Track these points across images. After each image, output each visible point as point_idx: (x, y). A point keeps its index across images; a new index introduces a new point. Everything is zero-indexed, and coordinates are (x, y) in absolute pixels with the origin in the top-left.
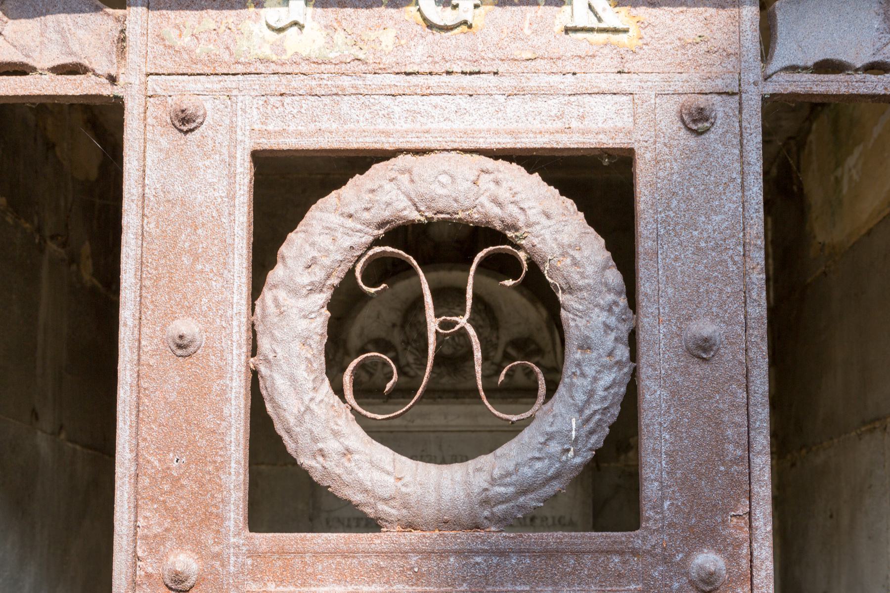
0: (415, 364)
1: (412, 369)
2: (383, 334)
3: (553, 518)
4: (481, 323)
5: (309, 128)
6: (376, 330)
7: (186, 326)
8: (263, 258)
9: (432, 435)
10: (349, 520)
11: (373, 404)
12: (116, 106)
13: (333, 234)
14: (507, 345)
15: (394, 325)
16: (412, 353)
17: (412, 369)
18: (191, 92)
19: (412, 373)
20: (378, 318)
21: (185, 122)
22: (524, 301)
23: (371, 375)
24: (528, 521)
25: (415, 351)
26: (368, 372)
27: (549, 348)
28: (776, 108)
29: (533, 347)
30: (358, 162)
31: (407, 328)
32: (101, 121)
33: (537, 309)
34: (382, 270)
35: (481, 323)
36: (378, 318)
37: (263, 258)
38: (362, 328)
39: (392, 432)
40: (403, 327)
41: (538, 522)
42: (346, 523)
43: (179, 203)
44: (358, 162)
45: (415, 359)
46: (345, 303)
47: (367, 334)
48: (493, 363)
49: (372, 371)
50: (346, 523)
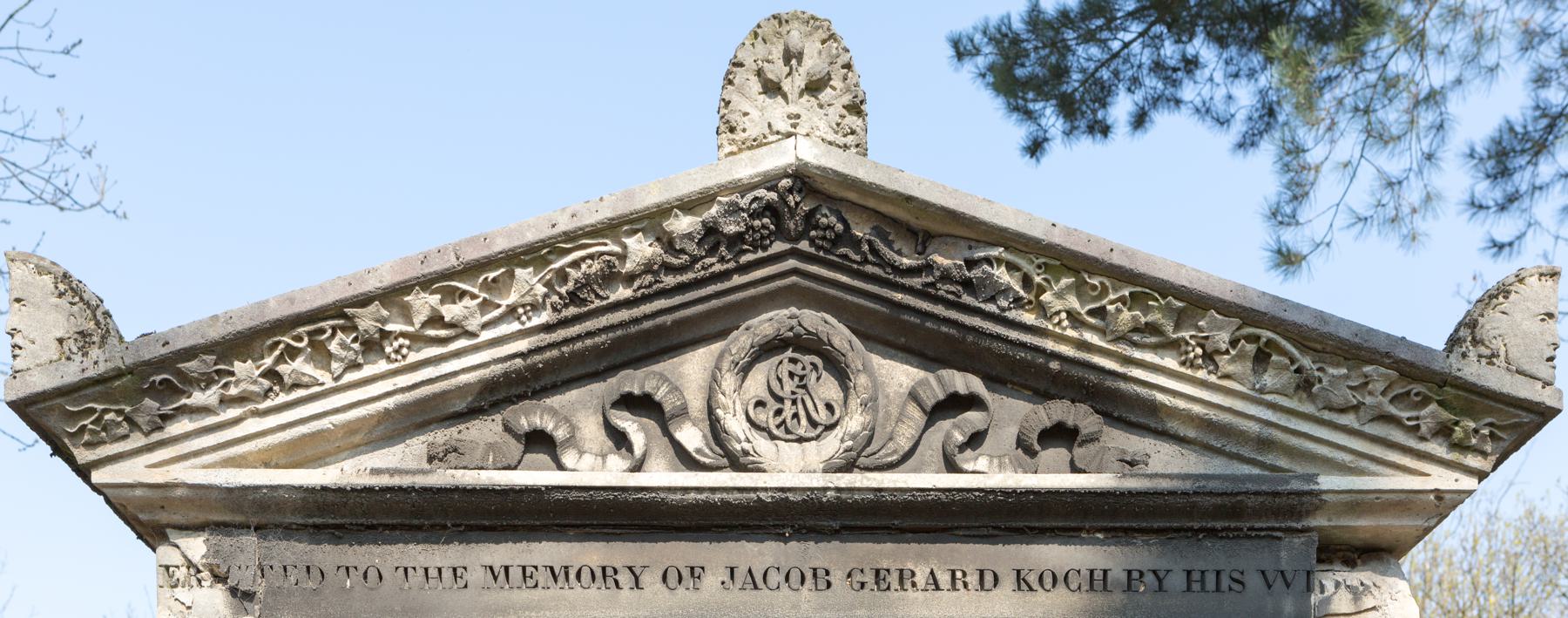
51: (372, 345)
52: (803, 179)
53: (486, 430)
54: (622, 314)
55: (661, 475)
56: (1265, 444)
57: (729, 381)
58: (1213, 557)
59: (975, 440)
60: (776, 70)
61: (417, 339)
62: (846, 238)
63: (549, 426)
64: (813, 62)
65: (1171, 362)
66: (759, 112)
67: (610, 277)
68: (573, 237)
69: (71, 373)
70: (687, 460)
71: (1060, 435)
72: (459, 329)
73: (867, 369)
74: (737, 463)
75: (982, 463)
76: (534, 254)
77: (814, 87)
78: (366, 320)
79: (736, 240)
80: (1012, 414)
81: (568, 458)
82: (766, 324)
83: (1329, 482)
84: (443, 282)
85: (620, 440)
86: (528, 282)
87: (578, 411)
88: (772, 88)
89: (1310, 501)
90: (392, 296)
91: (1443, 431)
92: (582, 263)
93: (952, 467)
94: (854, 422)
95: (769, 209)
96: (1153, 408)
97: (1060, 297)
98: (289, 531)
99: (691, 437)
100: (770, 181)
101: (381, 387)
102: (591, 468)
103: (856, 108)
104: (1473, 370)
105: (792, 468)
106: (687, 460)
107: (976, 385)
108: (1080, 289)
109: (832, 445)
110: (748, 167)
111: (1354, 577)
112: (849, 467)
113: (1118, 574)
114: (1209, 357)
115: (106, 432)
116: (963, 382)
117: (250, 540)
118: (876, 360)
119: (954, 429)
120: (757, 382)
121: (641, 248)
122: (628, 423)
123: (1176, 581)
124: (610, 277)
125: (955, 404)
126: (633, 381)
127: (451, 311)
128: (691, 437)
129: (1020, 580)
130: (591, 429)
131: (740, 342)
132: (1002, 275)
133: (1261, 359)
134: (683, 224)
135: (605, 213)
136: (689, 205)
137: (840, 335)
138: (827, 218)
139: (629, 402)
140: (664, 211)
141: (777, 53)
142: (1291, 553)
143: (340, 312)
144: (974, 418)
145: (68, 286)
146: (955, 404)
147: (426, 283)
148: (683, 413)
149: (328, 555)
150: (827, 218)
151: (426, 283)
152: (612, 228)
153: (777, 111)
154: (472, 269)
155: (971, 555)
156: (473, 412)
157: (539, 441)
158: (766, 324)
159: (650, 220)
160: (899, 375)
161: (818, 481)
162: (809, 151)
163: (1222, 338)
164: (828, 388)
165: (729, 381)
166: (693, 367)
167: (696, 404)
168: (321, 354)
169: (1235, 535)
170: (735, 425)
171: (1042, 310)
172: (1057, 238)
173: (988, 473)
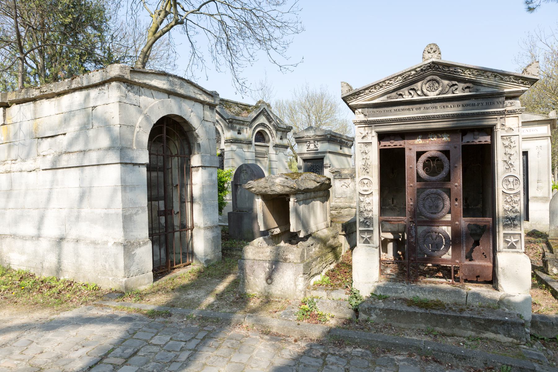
5: (420, 150)
7: (411, 166)
8: (417, 160)
12: (404, 148)
13: (423, 158)
18: (411, 147)
21: (410, 149)
28: (463, 146)
30: (425, 152)
32: (403, 150)
34: (427, 161)
37: (417, 160)
43: (410, 155)
44: (425, 152)
46: (424, 163)
47: (426, 166)
51: (381, 87)
52: (433, 63)
53: (394, 94)
54: (410, 80)
55: (416, 98)
56: (496, 86)
57: (424, 86)
58: (489, 101)
59: (456, 89)
60: (430, 51)
61: (386, 86)
62: (439, 68)
63: (402, 93)
64: (434, 49)
65: (483, 78)
66: (427, 55)
67: (409, 76)
68: (405, 73)
69: (348, 94)
70: (419, 95)
71: (468, 87)
72: (391, 84)
73: (442, 82)
74: (425, 95)
75: (457, 92)
76: (400, 75)
77: (434, 52)
78: (381, 85)
79: (425, 70)
80: (461, 85)
81: (404, 96)
82: (428, 78)
83: (506, 90)
84: (390, 79)
85: (410, 94)
86: (400, 78)
87: (405, 91)
88: (429, 53)
89: (504, 93)
90: (384, 82)
91: (522, 83)
92: (406, 75)
93: (453, 93)
94: (440, 89)
95: (429, 66)
96: (481, 83)
97: (467, 72)
98: (371, 108)
99: (419, 92)
100: (429, 63)
101: (382, 91)
102: (407, 98)
103: (440, 54)
104: (526, 75)
105: (432, 95)
106: (419, 95)
107: (456, 83)
108: (470, 71)
109: (437, 92)
110: (426, 62)
111: (511, 101)
112: (439, 94)
113: (476, 104)
114: (488, 77)
115: (352, 99)
116: (454, 82)
117: (366, 109)
118: (443, 81)
119: (453, 88)
120: (427, 85)
121: (413, 72)
122: (411, 92)
123: (485, 104)
124: (409, 76)
125: (453, 85)
126: (412, 87)
127: (390, 82)
128: (419, 92)
129: (463, 106)
130: (407, 93)
131: (425, 81)
132: (459, 70)
133: (495, 76)
134: (418, 69)
135: (409, 70)
136: (419, 67)
137: (438, 78)
138: (436, 66)
139: (411, 89)
140: (416, 68)
141: (430, 48)
142: (501, 99)
143: (378, 84)
144: (456, 87)
145: (348, 85)
146: (453, 85)
147: (388, 80)
148: (418, 90)
149: (375, 110)
150: (436, 66)
151: (388, 80)
152: (410, 71)
153: (430, 55)
154: (393, 78)
155: (456, 103)
156: (392, 92)
157: (401, 95)
158: (428, 78)
159: (414, 70)
160: (446, 82)
161: (436, 97)
162: (434, 60)
163: (490, 75)
164: (437, 85)
165: (424, 86)
166: (419, 84)
167: (420, 88)
168: (375, 88)
169: (493, 98)
170: (425, 90)
171: (465, 74)
172: (466, 66)
173: (459, 93)
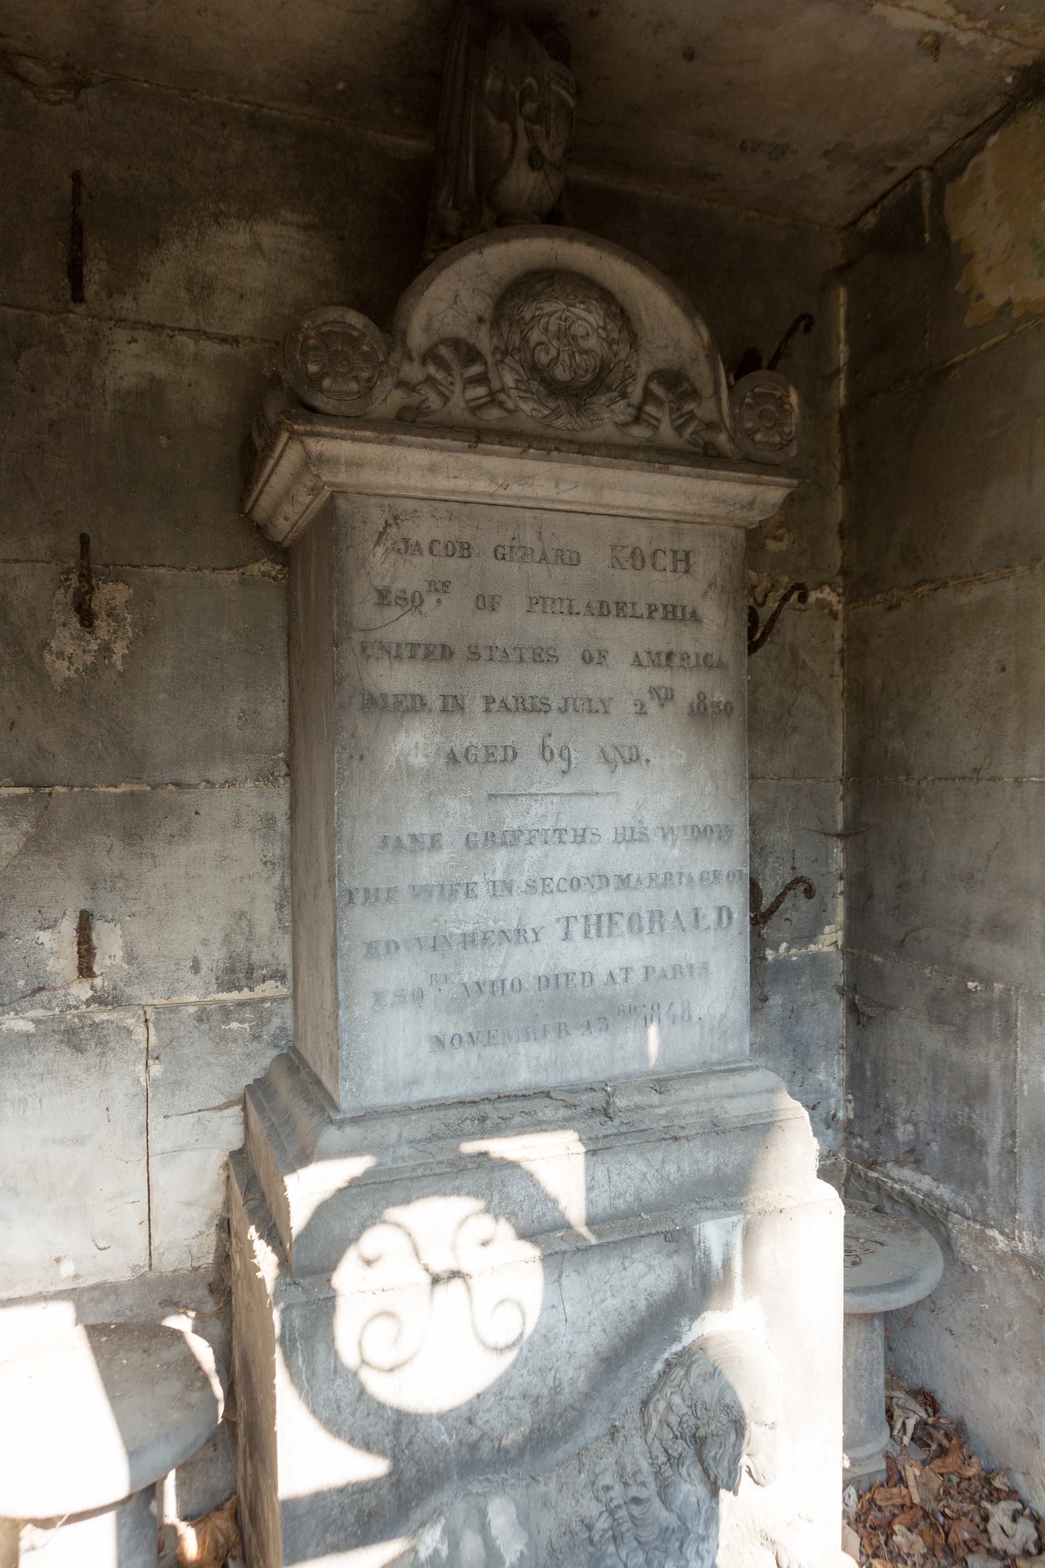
0: (517, 388)
1: (509, 397)
2: (463, 333)
3: (697, 655)
4: (615, 335)
6: (454, 325)
9: (528, 514)
10: (398, 645)
11: (450, 450)
14: (649, 379)
15: (481, 320)
16: (513, 369)
17: (509, 397)
19: (510, 405)
20: (455, 302)
22: (675, 310)
23: (446, 400)
24: (663, 657)
25: (518, 367)
26: (440, 393)
27: (708, 391)
29: (686, 385)
31: (505, 328)
33: (694, 325)
35: (615, 335)
36: (455, 302)
38: (430, 317)
39: (466, 503)
40: (495, 323)
41: (676, 660)
42: (394, 652)
45: (517, 381)
48: (629, 405)
49: (447, 393)
50: (394, 652)
